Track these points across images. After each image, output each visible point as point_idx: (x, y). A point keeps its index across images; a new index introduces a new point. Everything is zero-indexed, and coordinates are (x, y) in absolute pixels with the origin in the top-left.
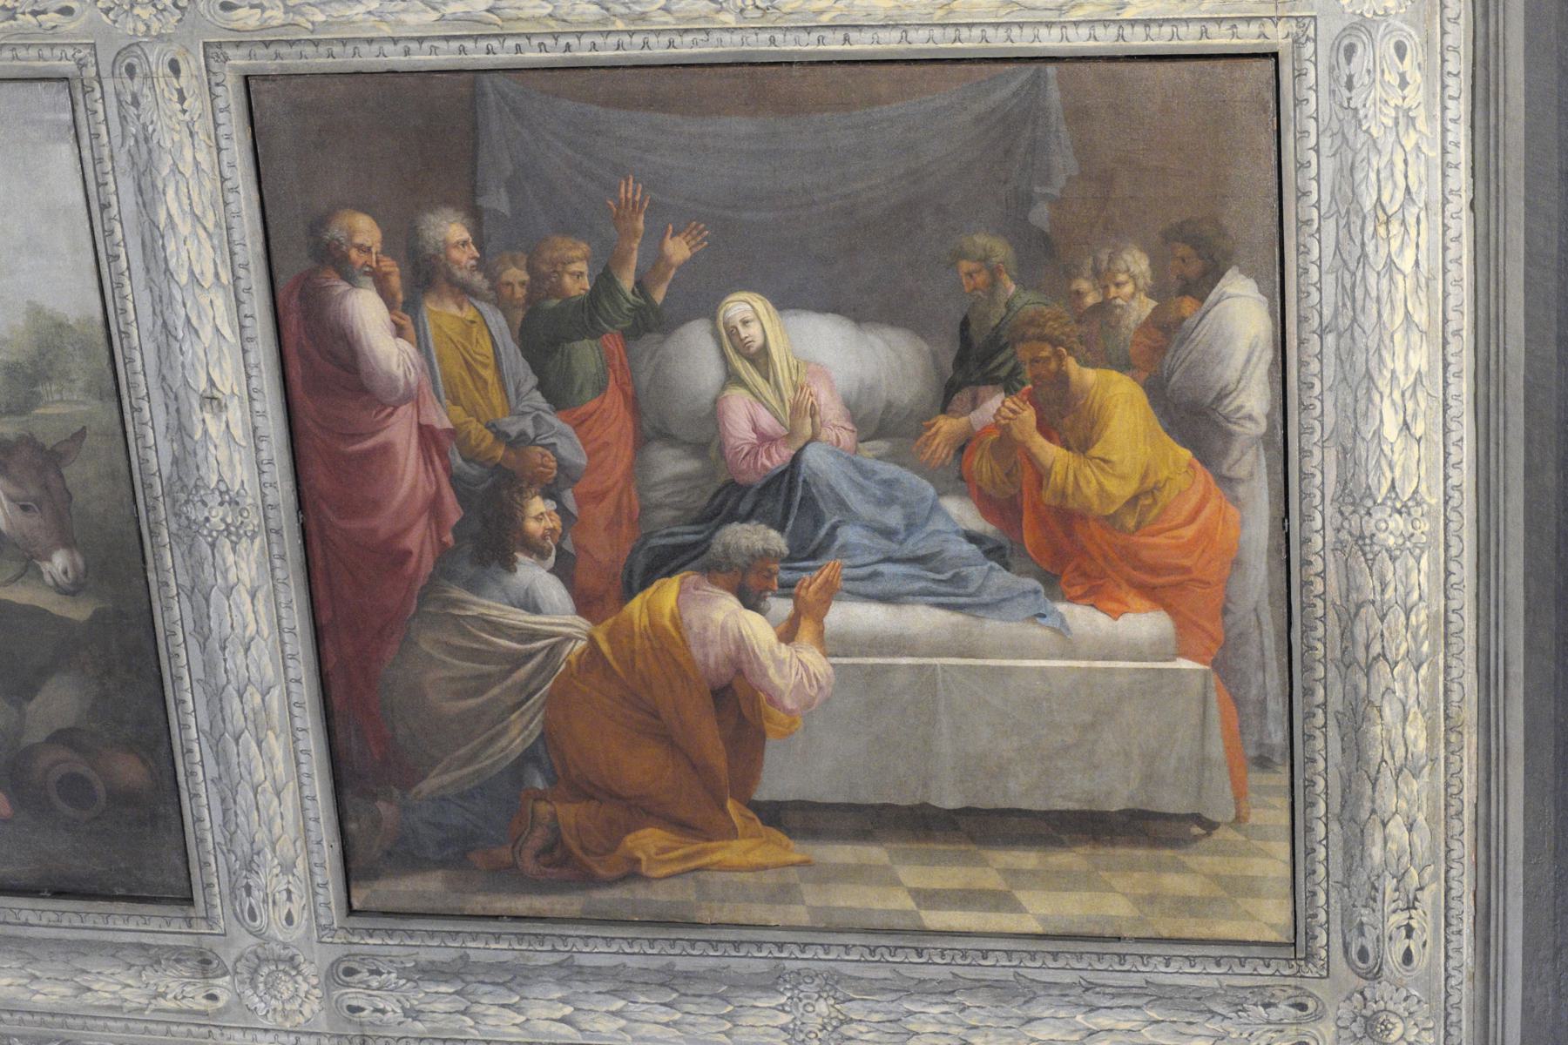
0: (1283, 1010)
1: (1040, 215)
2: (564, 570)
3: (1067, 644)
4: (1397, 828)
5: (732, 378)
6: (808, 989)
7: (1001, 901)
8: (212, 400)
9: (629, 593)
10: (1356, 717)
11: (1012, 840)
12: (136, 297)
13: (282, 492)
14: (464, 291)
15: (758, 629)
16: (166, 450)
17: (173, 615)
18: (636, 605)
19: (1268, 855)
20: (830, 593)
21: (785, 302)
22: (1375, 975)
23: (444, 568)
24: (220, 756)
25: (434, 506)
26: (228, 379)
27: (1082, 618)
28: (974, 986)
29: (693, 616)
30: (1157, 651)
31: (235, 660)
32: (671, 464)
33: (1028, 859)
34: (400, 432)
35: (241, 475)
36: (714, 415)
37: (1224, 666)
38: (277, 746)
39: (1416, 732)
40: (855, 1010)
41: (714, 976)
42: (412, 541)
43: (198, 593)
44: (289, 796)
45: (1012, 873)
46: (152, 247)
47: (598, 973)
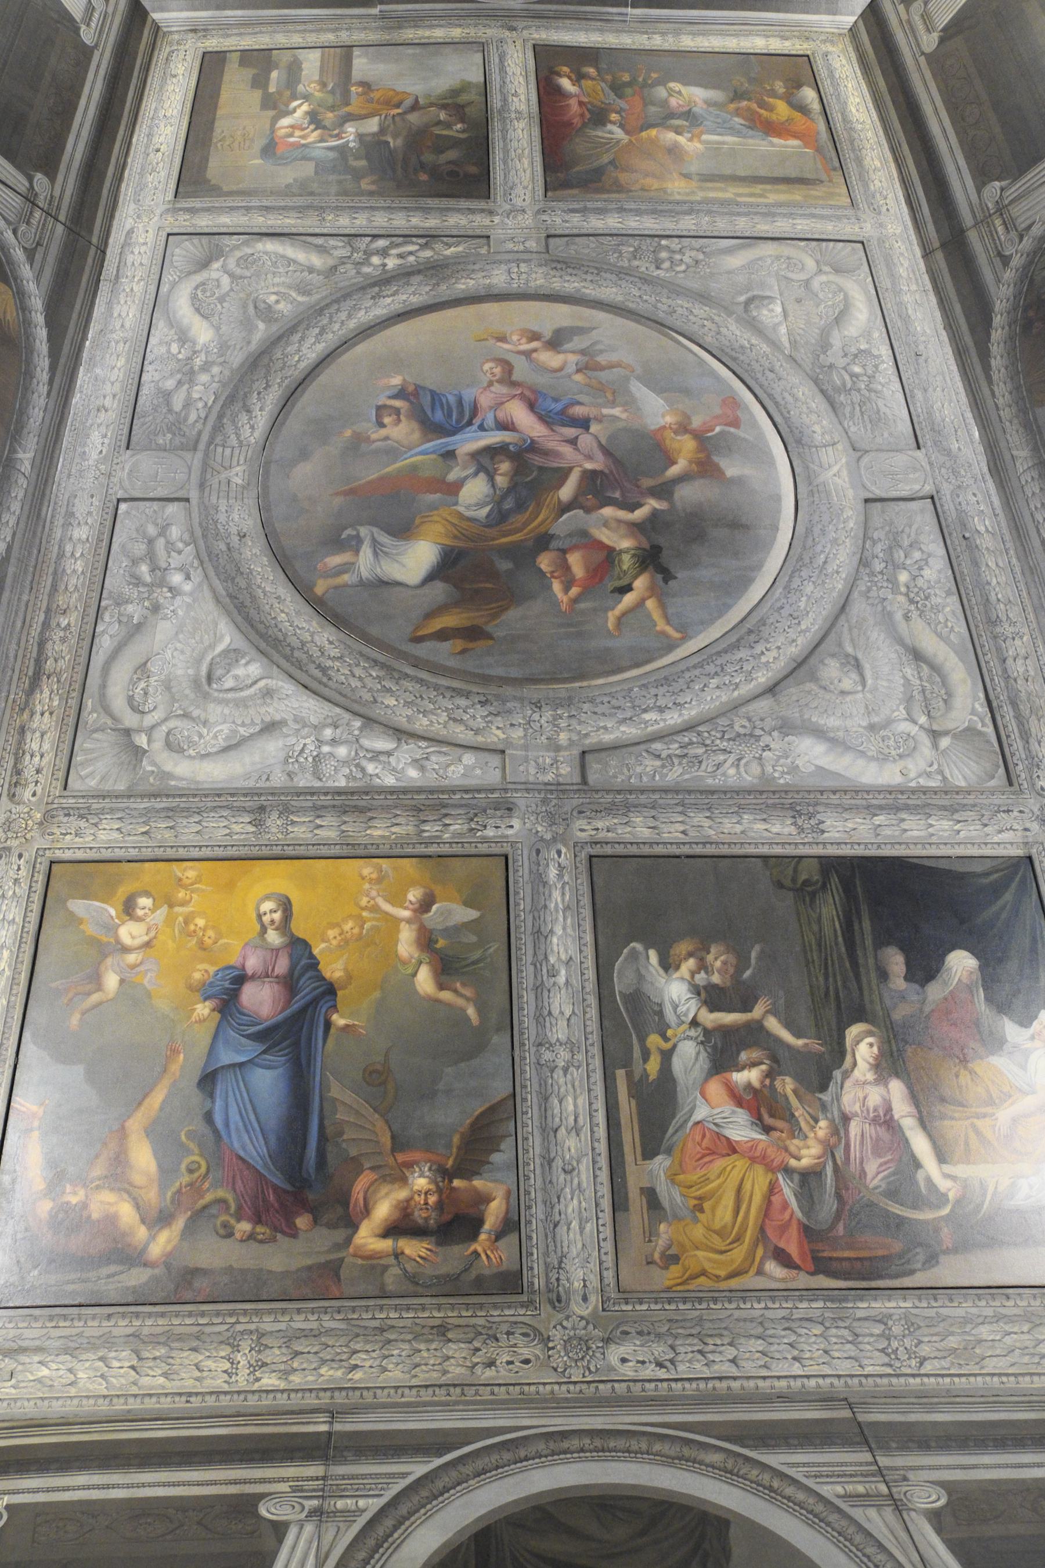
0: (853, 220)
1: (753, 75)
2: (622, 126)
3: (773, 145)
4: (876, 182)
5: (671, 95)
6: (702, 214)
7: (761, 196)
8: (516, 95)
9: (642, 130)
10: (859, 161)
11: (762, 183)
12: (495, 78)
13: (535, 108)
14: (593, 79)
15: (681, 140)
16: (499, 104)
17: (496, 135)
18: (644, 134)
19: (840, 195)
20: (702, 133)
21: (685, 84)
22: (880, 213)
23: (584, 125)
24: (505, 163)
25: (582, 115)
26: (522, 90)
27: (776, 140)
28: (756, 213)
29: (661, 136)
30: (799, 147)
31: (515, 144)
32: (653, 109)
33: (769, 187)
34: (573, 102)
35: (523, 107)
36: (666, 101)
37: (819, 150)
38: (526, 162)
39: (877, 163)
40: (717, 219)
41: (671, 211)
42: (575, 121)
43: (504, 131)
44: (528, 172)
45: (765, 190)
46: (502, 69)
47: (631, 210)
